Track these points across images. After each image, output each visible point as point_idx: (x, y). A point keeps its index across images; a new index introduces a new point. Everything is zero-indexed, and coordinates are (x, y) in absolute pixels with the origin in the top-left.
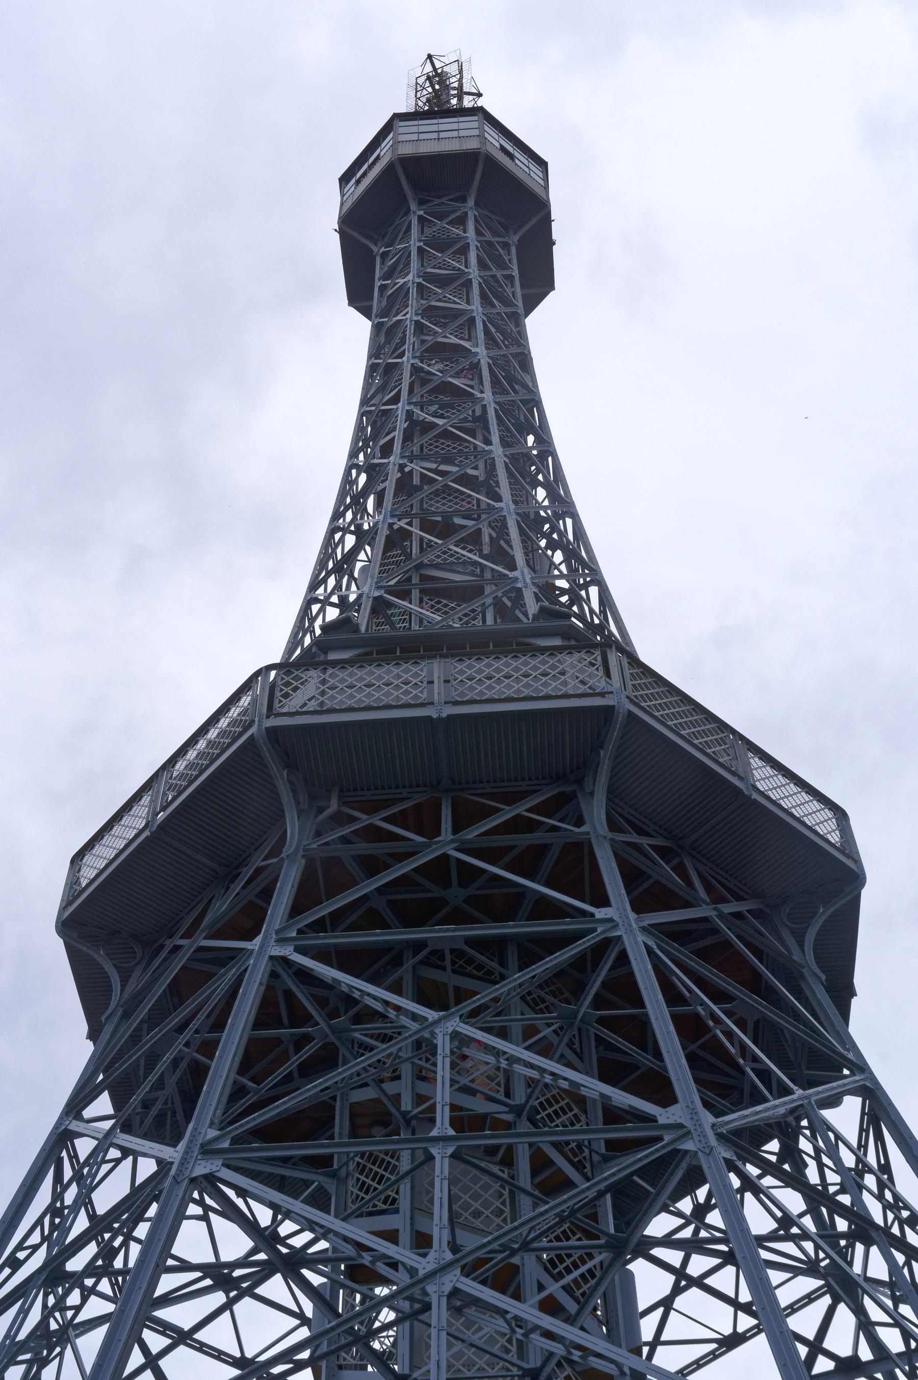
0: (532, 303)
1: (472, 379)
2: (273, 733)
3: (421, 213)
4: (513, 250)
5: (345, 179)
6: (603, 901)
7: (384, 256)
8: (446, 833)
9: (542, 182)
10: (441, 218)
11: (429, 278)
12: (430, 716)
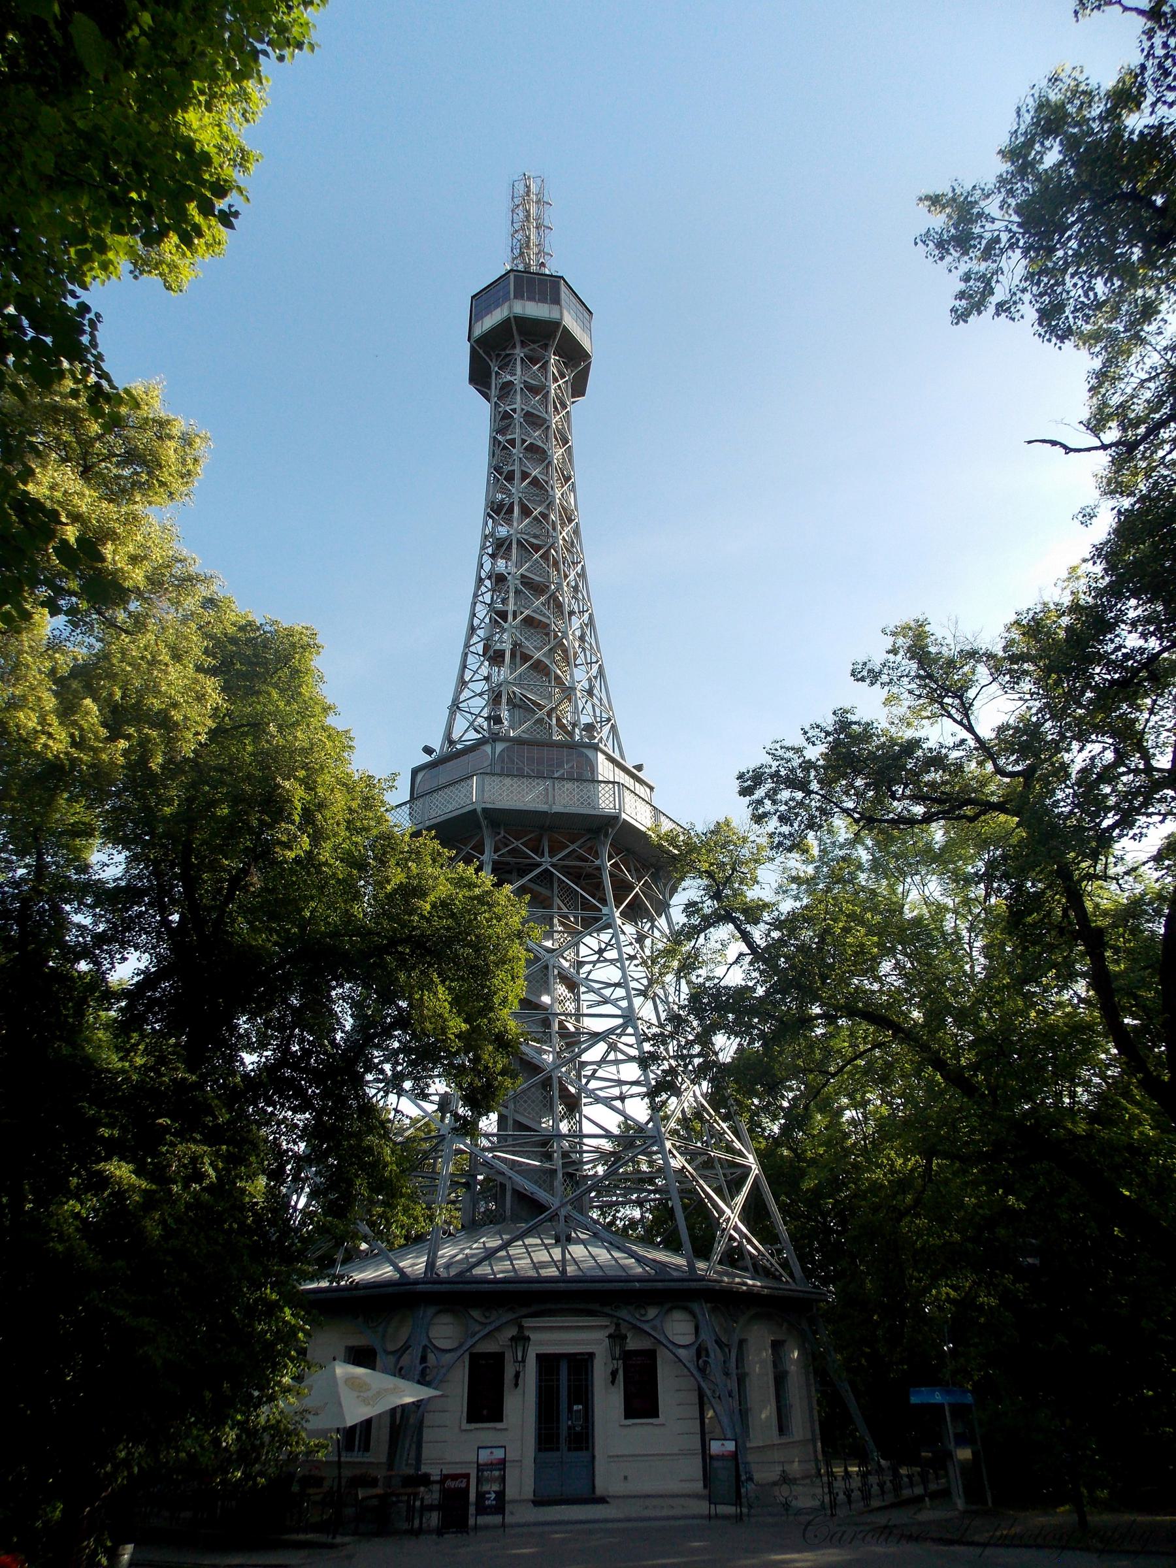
2: (484, 809)
6: (604, 901)
8: (547, 858)
11: (528, 415)
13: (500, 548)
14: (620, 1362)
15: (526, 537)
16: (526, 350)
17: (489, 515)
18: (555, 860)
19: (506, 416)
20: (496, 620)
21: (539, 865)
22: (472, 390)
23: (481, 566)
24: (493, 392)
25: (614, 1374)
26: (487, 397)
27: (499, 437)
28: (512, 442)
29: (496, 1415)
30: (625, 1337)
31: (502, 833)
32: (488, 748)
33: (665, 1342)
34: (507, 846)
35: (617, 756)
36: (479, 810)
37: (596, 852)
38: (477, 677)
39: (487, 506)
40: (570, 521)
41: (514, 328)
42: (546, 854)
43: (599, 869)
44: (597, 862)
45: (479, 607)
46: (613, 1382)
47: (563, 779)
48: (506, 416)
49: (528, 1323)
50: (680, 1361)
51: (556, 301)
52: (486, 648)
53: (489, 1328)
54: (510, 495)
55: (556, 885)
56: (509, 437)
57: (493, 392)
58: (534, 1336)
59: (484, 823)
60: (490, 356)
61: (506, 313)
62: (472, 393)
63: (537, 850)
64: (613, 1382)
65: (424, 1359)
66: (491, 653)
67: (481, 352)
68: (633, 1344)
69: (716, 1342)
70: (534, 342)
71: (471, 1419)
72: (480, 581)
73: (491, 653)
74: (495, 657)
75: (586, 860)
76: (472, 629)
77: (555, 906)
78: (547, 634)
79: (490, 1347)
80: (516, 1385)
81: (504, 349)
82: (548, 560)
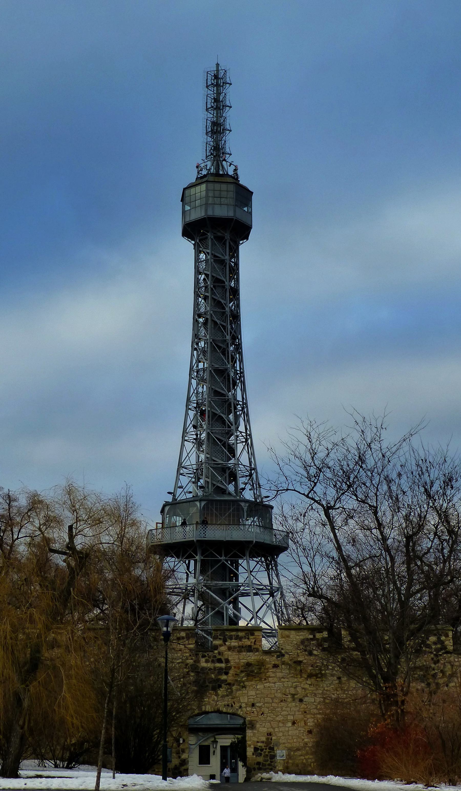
2: (197, 541)
5: (185, 189)
29: (208, 762)
42: (223, 555)
53: (206, 738)
61: (203, 214)
71: (200, 763)
79: (206, 743)
80: (214, 754)
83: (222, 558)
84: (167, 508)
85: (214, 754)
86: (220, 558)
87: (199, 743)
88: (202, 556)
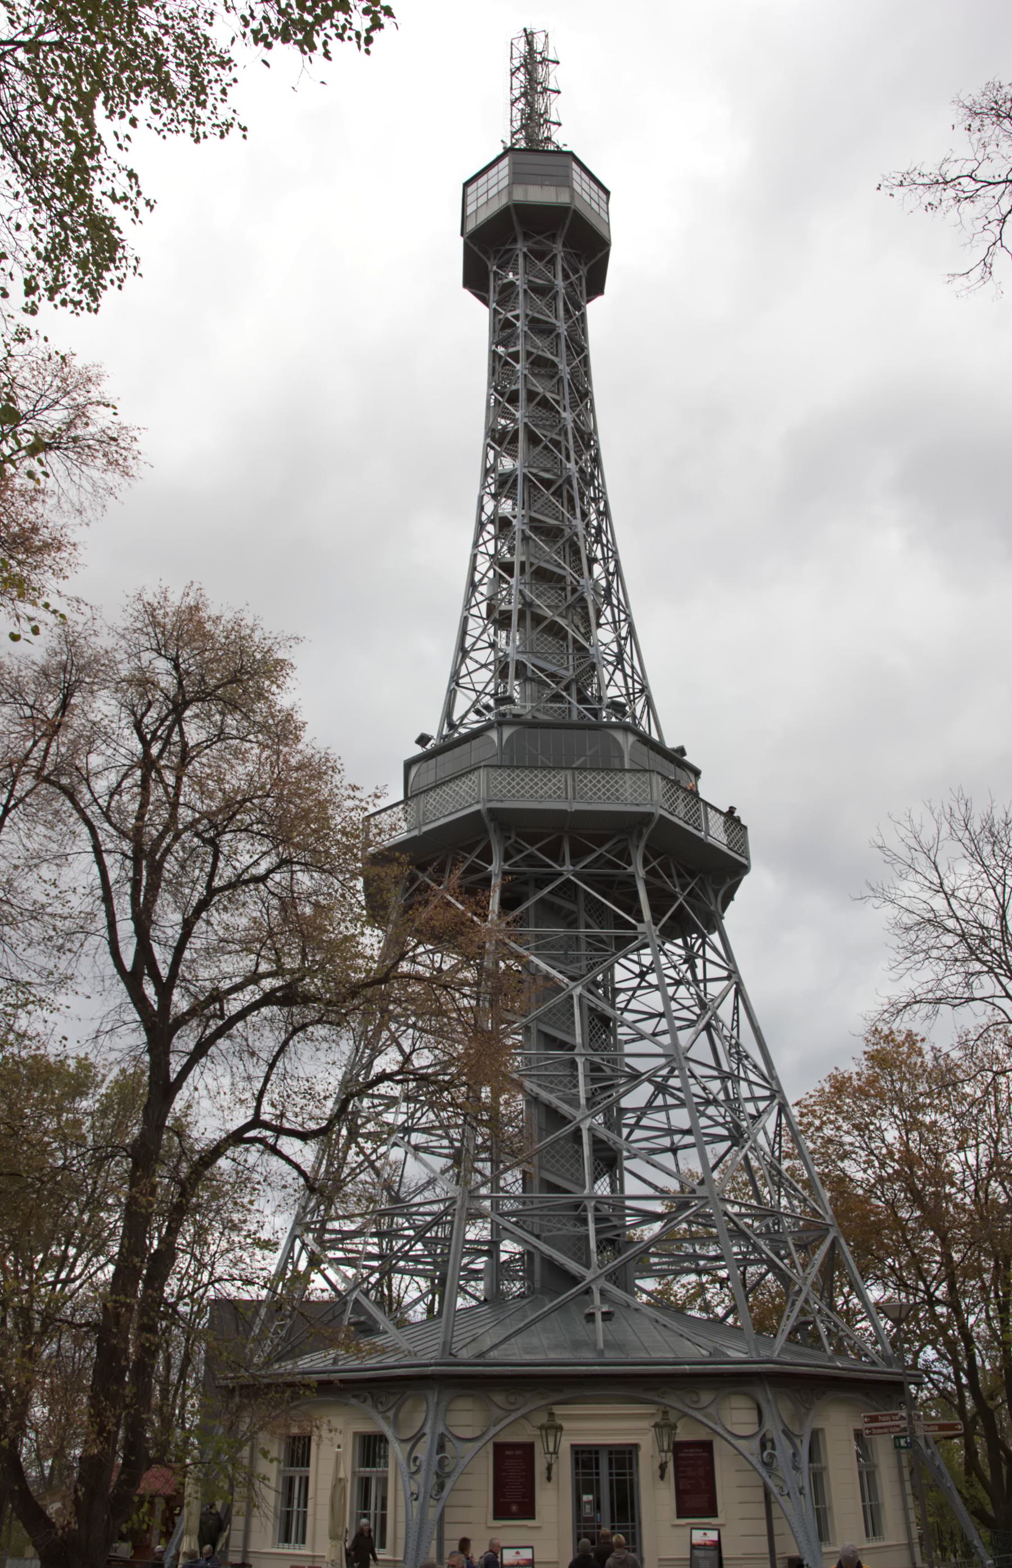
0: (588, 301)
1: (559, 434)
3: (525, 250)
4: (584, 280)
5: (467, 185)
6: (641, 920)
7: (496, 273)
8: (568, 867)
9: (603, 205)
10: (541, 259)
12: (565, 811)
13: (505, 485)
14: (670, 1455)
15: (534, 471)
16: (530, 243)
17: (489, 445)
18: (578, 868)
19: (508, 324)
20: (501, 576)
21: (561, 874)
22: (467, 294)
23: (481, 508)
24: (492, 296)
25: (663, 1467)
26: (485, 301)
27: (501, 350)
28: (515, 356)
29: (528, 1511)
30: (675, 1427)
31: (513, 838)
32: (494, 735)
33: (722, 1432)
34: (520, 852)
35: (655, 736)
36: (484, 813)
37: (629, 855)
38: (480, 644)
39: (487, 436)
40: (588, 447)
41: (515, 218)
43: (632, 876)
44: (630, 870)
45: (480, 559)
46: (662, 1477)
47: (585, 769)
48: (508, 324)
49: (559, 1410)
50: (741, 1453)
51: (566, 182)
52: (490, 609)
54: (514, 420)
55: (581, 897)
56: (511, 350)
57: (492, 296)
58: (566, 1425)
59: (491, 826)
60: (485, 253)
62: (469, 298)
63: (559, 859)
64: (662, 1477)
65: (441, 1448)
66: (496, 615)
67: (476, 249)
68: (683, 1434)
69: (784, 1432)
70: (539, 233)
72: (481, 526)
73: (496, 615)
74: (501, 620)
75: (618, 867)
76: (473, 586)
77: (582, 923)
78: (564, 589)
80: (549, 1479)
81: (504, 244)
82: (561, 496)
83: (564, 868)
84: (414, 771)
85: (549, 1479)
86: (558, 868)
87: (493, 1431)
88: (505, 861)
